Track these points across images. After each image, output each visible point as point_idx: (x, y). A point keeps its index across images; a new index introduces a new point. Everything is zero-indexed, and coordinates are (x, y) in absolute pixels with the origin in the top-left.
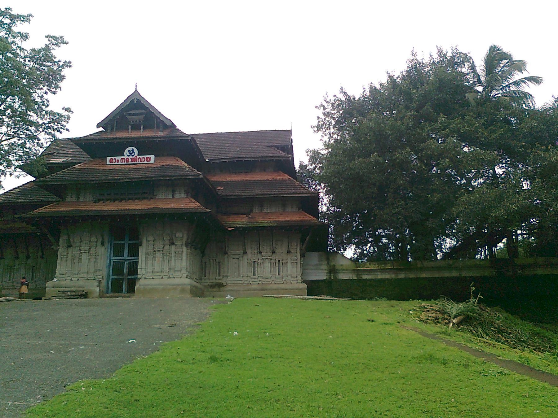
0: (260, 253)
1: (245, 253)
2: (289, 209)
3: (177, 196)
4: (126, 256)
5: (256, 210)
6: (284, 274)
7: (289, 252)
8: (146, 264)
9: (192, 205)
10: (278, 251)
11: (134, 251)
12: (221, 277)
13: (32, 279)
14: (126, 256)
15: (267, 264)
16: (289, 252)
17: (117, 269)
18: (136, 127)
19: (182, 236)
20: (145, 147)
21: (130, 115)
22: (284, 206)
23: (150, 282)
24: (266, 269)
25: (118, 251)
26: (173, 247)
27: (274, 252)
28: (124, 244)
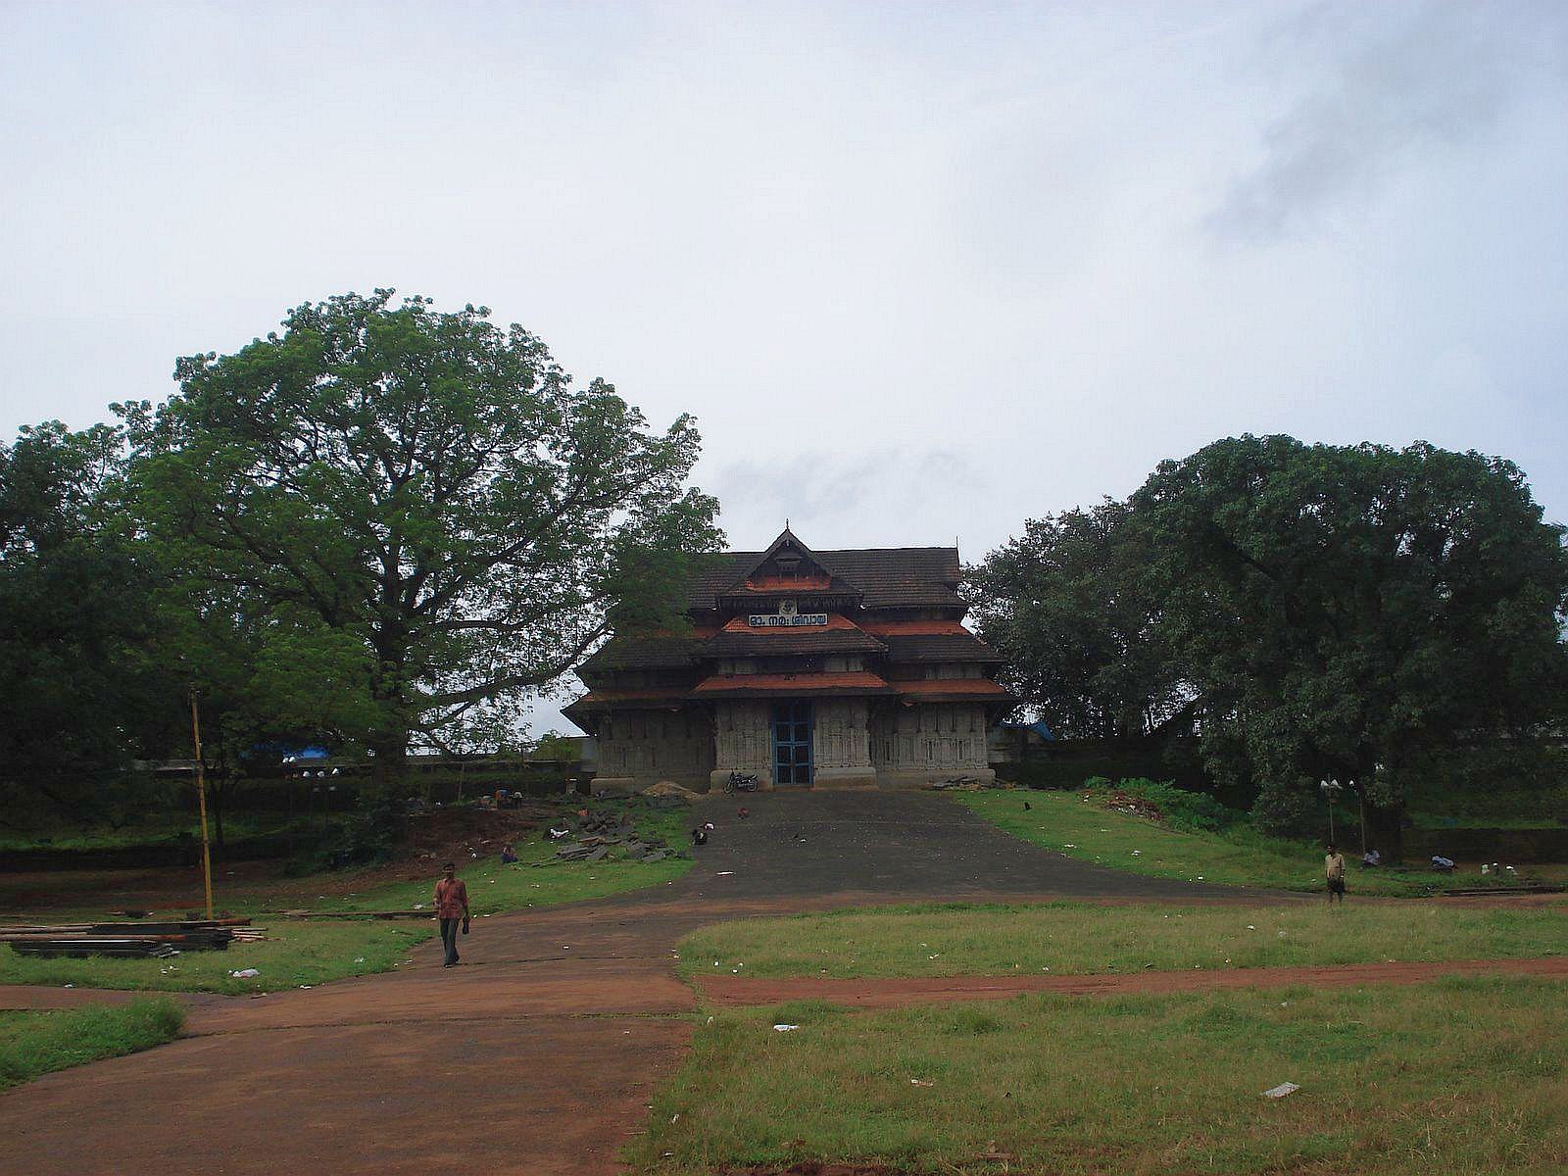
0: (937, 731)
1: (919, 731)
2: (970, 675)
3: (852, 669)
4: (792, 740)
5: (930, 676)
6: (968, 757)
7: (972, 730)
8: (822, 751)
9: (873, 682)
10: (960, 728)
11: (804, 734)
12: (890, 762)
13: (654, 765)
14: (792, 740)
15: (946, 745)
16: (972, 730)
17: (782, 754)
18: (788, 574)
19: (862, 716)
20: (806, 604)
21: (781, 560)
22: (964, 670)
23: (825, 771)
24: (945, 752)
25: (782, 734)
26: (852, 730)
27: (953, 731)
28: (787, 727)
